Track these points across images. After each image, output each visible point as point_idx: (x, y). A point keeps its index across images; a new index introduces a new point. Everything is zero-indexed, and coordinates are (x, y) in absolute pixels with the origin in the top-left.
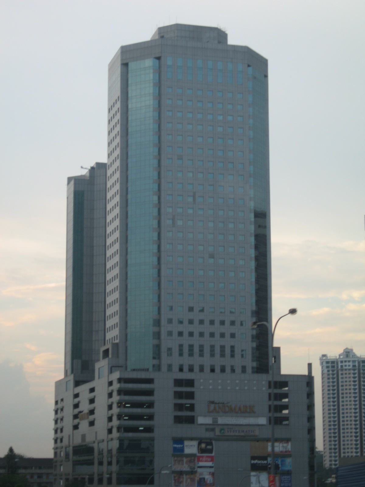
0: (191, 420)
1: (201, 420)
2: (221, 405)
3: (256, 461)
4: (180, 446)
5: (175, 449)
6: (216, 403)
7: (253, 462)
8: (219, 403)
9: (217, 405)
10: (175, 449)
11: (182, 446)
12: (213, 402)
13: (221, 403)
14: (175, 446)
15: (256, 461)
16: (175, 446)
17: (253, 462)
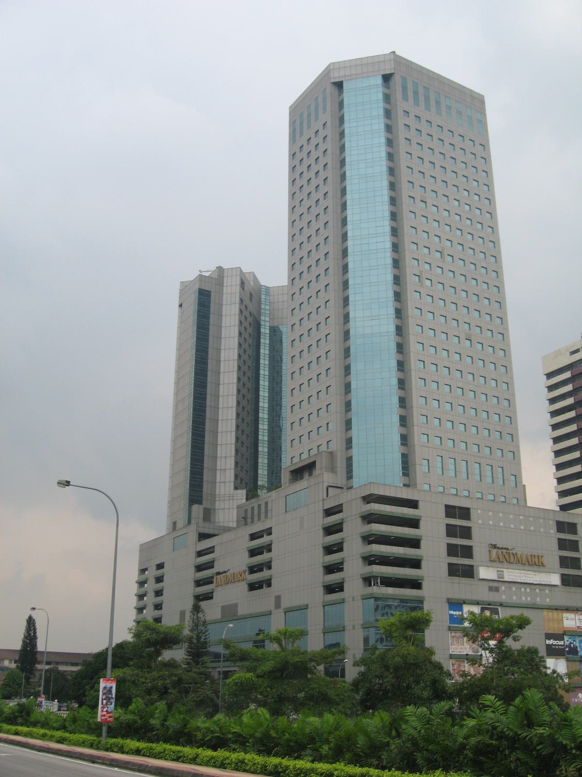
0: (469, 572)
1: (484, 573)
2: (504, 551)
3: (551, 642)
4: (457, 613)
5: (452, 619)
6: (499, 548)
7: (548, 642)
8: (502, 548)
9: (500, 551)
10: (452, 619)
11: (460, 613)
12: (495, 546)
13: (505, 549)
14: (452, 612)
15: (551, 642)
16: (452, 612)
17: (548, 642)
